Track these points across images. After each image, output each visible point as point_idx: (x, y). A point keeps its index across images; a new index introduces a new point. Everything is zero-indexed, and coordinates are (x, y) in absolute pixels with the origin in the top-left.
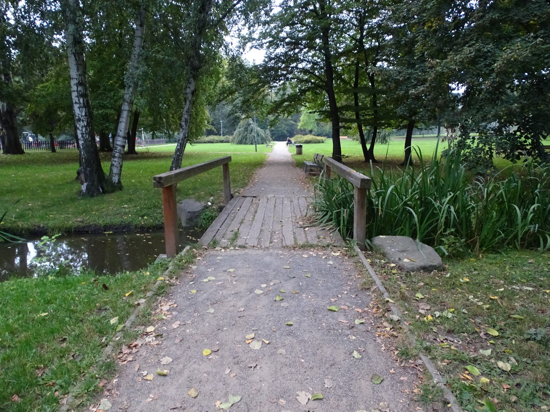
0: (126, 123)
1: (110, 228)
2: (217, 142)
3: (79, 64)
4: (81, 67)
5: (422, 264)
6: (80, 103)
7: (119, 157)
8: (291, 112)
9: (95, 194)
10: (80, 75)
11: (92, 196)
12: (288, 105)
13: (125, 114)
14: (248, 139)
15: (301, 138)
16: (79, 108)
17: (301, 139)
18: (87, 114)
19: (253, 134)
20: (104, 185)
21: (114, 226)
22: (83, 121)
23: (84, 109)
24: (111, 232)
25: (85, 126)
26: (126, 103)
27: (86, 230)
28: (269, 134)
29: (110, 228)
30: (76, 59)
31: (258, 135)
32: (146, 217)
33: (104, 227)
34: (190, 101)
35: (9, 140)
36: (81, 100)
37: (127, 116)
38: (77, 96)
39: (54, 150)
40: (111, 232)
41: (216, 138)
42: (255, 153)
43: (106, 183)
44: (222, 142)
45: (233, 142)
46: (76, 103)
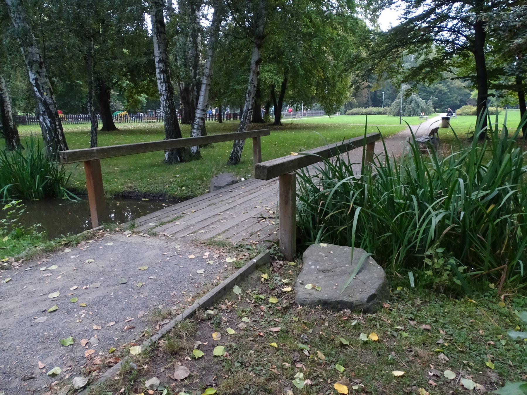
0: (205, 96)
1: (149, 195)
2: (375, 114)
3: (160, 43)
4: (162, 46)
5: (325, 296)
6: (161, 79)
7: (198, 129)
8: (433, 80)
9: (173, 163)
10: (161, 53)
11: (171, 163)
12: (429, 71)
13: (203, 87)
14: (406, 111)
15: (469, 108)
16: (160, 83)
17: (469, 110)
18: (167, 88)
19: (412, 105)
20: (183, 154)
21: (153, 193)
22: (163, 95)
23: (164, 84)
24: (147, 199)
25: (165, 100)
26: (205, 77)
27: (130, 195)
28: (431, 105)
29: (149, 195)
30: (158, 39)
31: (418, 106)
32: (184, 188)
33: (144, 194)
34: (254, 72)
35: (185, 113)
36: (162, 76)
37: (206, 90)
38: (159, 73)
39: (221, 121)
40: (147, 199)
41: (375, 109)
42: (399, 125)
43: (185, 153)
44: (380, 113)
45: (390, 113)
46: (158, 79)
